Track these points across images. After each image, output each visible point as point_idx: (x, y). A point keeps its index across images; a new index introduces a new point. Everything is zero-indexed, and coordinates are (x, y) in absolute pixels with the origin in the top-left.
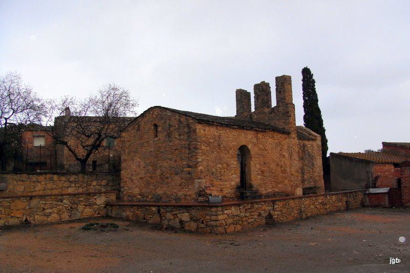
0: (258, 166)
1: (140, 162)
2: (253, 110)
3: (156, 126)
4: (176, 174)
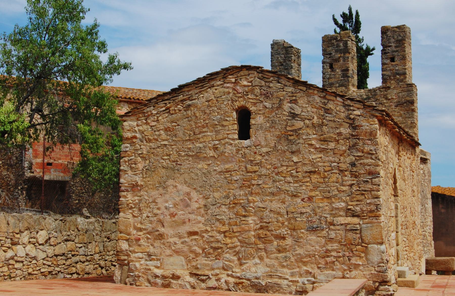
1: (188, 194)
4: (313, 230)
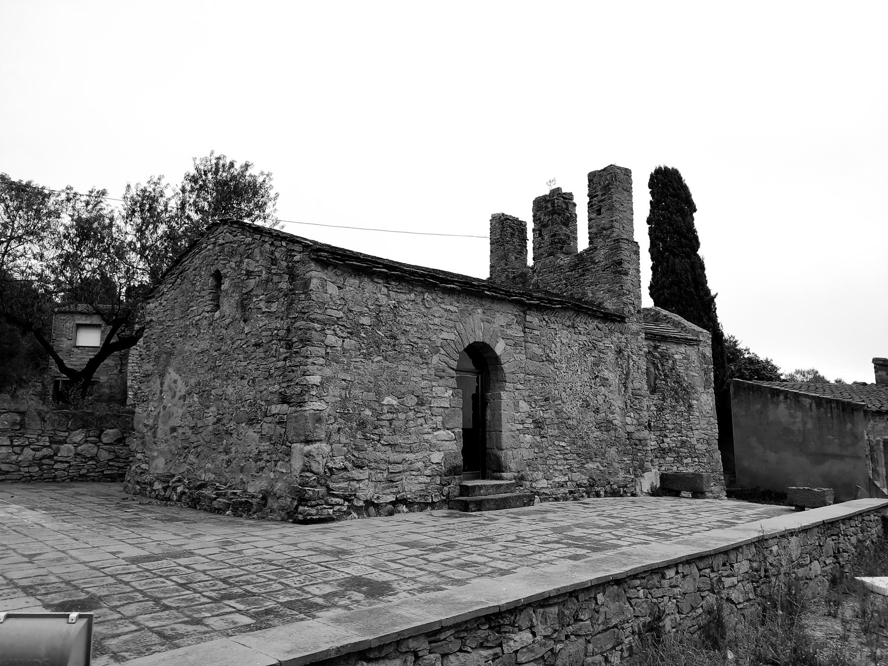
0: (524, 406)
1: (175, 382)
2: (530, 262)
3: (218, 277)
4: (251, 422)
